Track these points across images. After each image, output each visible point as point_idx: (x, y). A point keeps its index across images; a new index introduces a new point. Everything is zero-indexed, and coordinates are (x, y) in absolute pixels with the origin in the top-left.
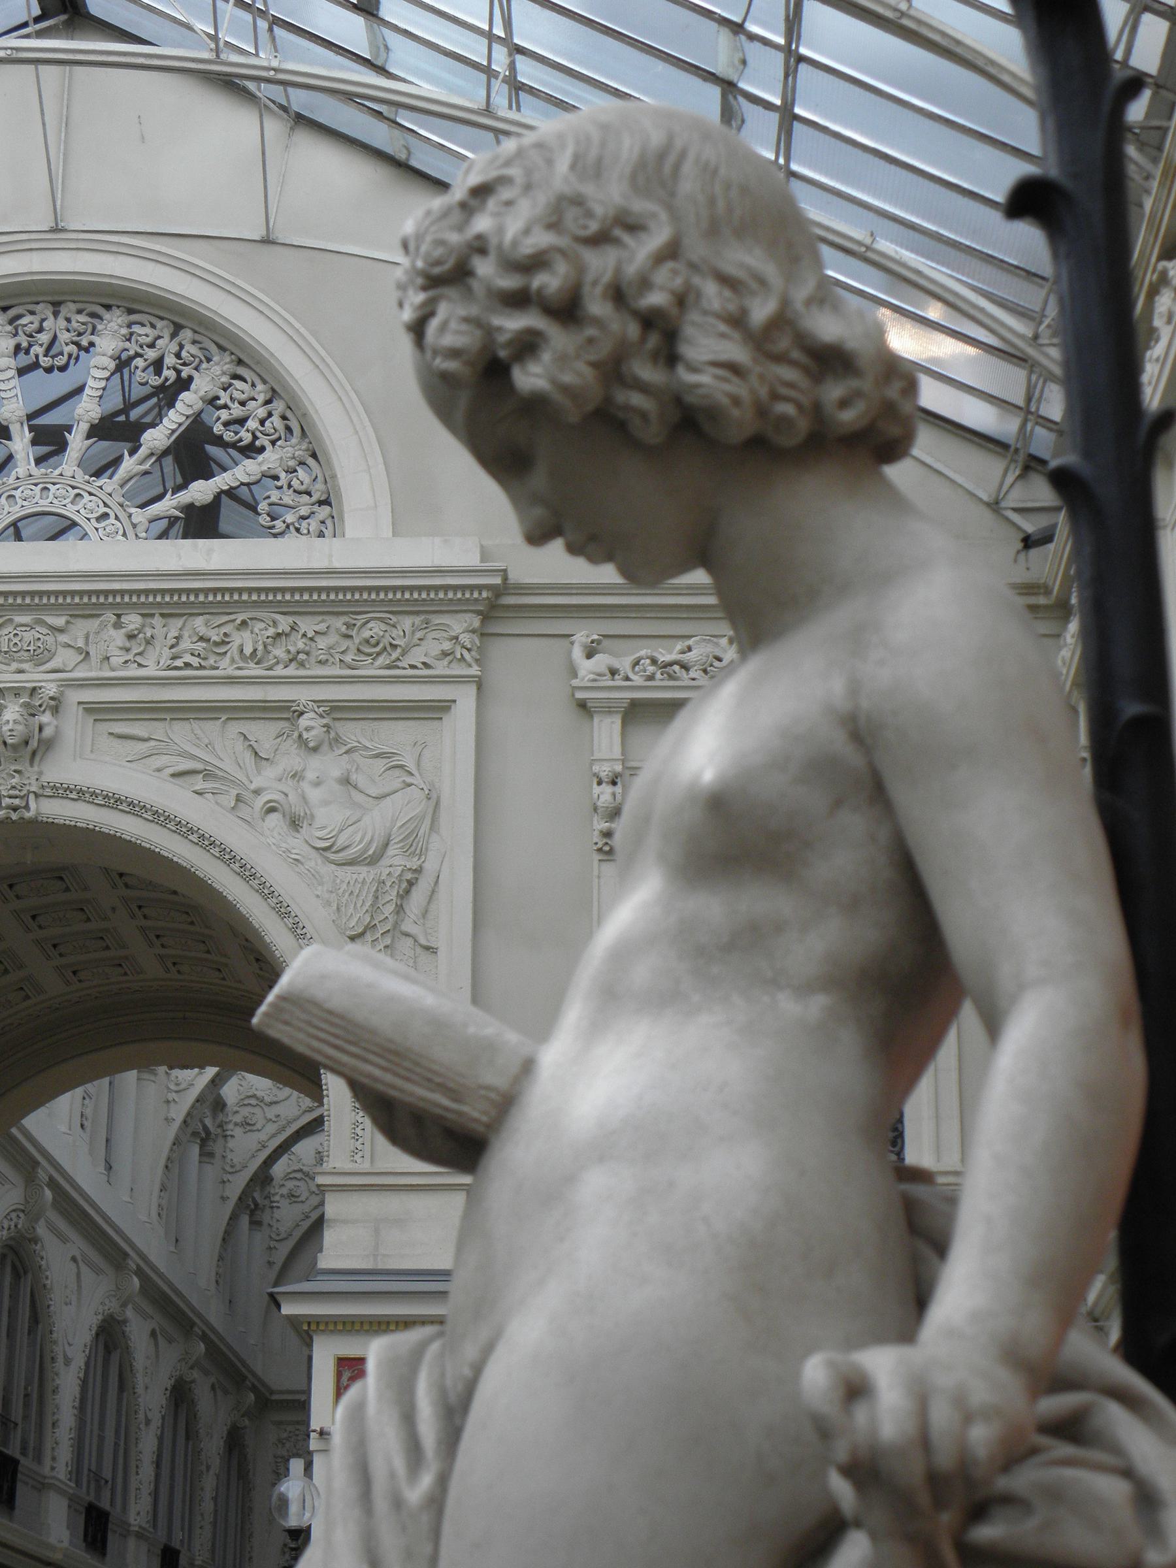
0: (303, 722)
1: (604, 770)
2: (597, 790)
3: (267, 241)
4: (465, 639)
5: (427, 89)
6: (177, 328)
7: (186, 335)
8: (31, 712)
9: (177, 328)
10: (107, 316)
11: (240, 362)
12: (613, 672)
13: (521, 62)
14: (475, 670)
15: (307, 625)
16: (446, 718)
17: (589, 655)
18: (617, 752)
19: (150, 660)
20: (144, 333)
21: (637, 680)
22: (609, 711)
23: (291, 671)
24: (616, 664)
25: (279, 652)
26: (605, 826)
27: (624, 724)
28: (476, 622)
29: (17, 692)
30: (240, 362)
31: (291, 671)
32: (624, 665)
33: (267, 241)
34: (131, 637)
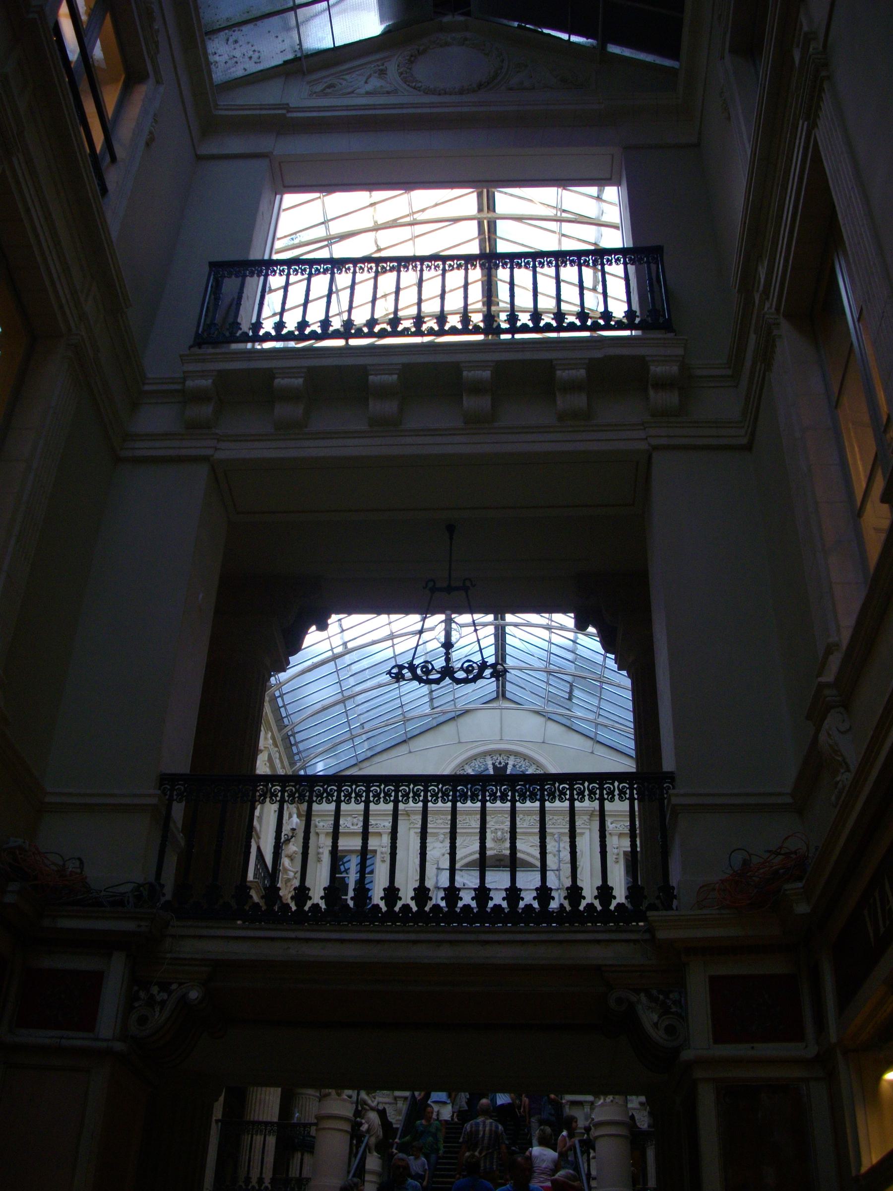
0: (556, 836)
1: (615, 846)
2: (614, 850)
3: (543, 742)
4: (587, 820)
5: (579, 714)
6: (525, 759)
7: (527, 761)
8: (503, 833)
9: (525, 759)
10: (510, 757)
11: (538, 766)
12: (616, 827)
13: (601, 711)
14: (589, 827)
15: (556, 817)
16: (584, 836)
17: (611, 824)
18: (617, 843)
19: (525, 824)
20: (518, 760)
21: (621, 829)
22: (616, 835)
23: (553, 826)
24: (617, 825)
25: (550, 823)
26: (616, 857)
27: (619, 837)
28: (589, 817)
29: (500, 829)
30: (538, 766)
31: (553, 826)
32: (618, 826)
33: (543, 742)
34: (521, 819)
